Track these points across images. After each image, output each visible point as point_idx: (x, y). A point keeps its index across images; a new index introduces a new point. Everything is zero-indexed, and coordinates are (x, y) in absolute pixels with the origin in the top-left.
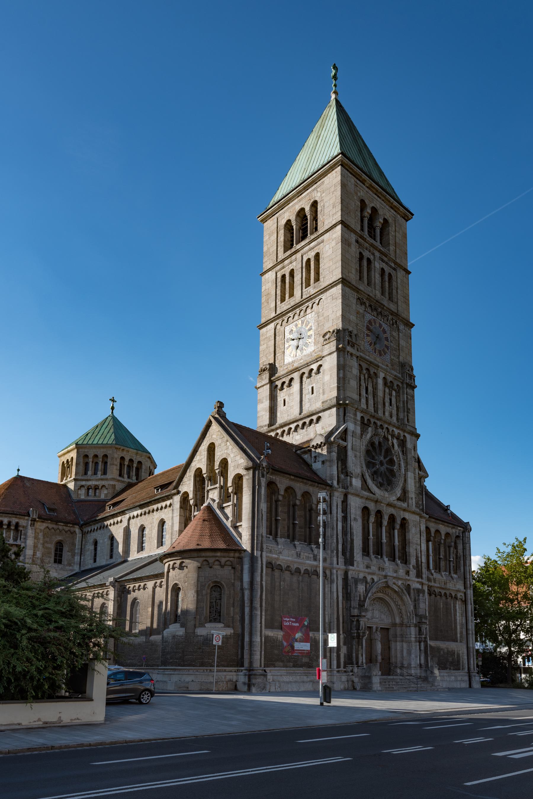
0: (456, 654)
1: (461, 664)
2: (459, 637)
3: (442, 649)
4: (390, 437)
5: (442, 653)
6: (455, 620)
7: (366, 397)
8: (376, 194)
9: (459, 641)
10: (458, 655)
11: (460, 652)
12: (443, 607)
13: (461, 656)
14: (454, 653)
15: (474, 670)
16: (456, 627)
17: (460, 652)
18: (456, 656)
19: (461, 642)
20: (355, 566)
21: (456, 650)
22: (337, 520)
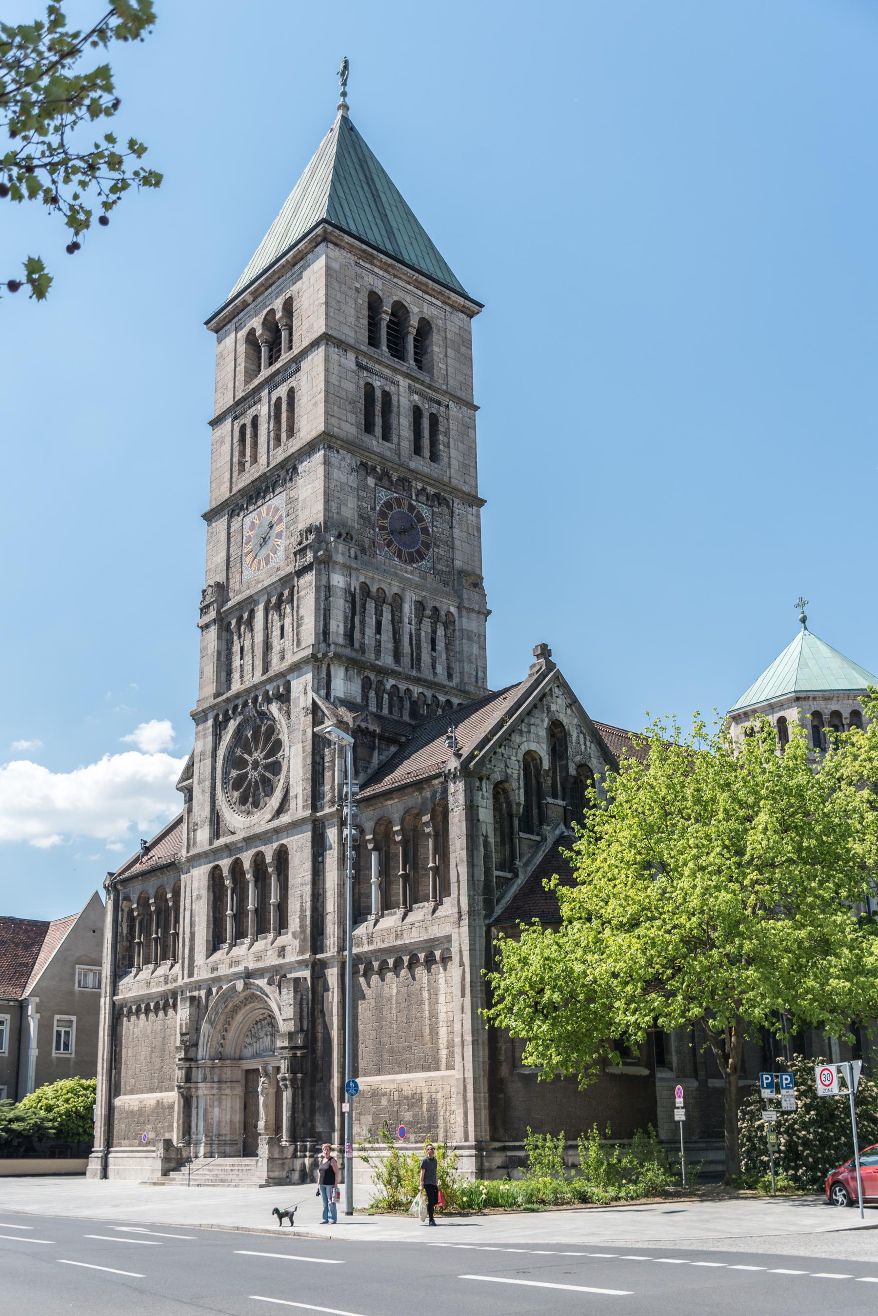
0: (425, 1101)
1: (442, 1126)
2: (444, 1056)
3: (385, 1094)
4: (264, 708)
5: (384, 1102)
6: (434, 1015)
7: (241, 665)
8: (267, 289)
9: (443, 1066)
10: (433, 1103)
11: (439, 1095)
12: (398, 992)
13: (440, 1103)
14: (422, 1098)
15: (467, 1140)
16: (434, 1032)
17: (439, 1095)
18: (425, 1107)
19: (450, 1067)
20: (195, 975)
21: (425, 1090)
22: (185, 909)
